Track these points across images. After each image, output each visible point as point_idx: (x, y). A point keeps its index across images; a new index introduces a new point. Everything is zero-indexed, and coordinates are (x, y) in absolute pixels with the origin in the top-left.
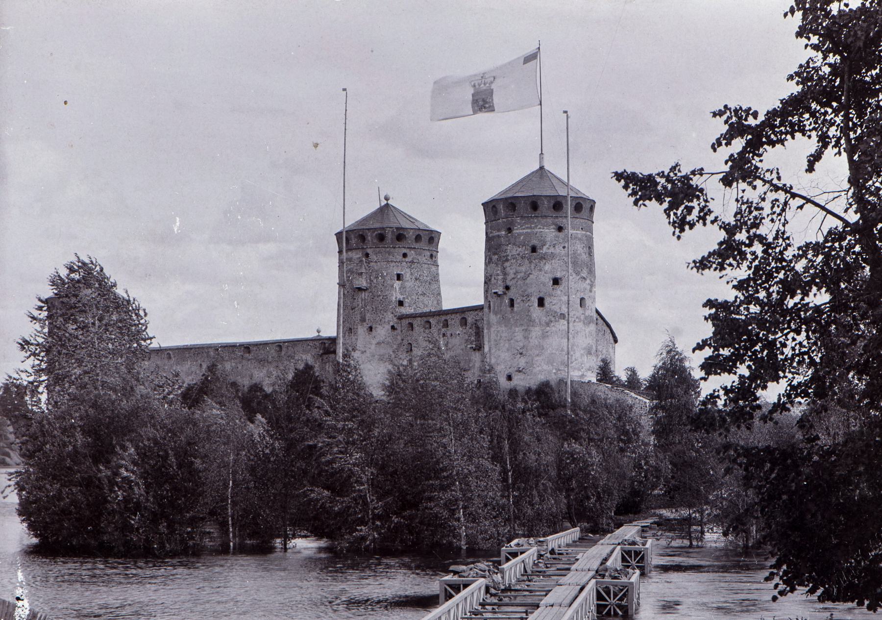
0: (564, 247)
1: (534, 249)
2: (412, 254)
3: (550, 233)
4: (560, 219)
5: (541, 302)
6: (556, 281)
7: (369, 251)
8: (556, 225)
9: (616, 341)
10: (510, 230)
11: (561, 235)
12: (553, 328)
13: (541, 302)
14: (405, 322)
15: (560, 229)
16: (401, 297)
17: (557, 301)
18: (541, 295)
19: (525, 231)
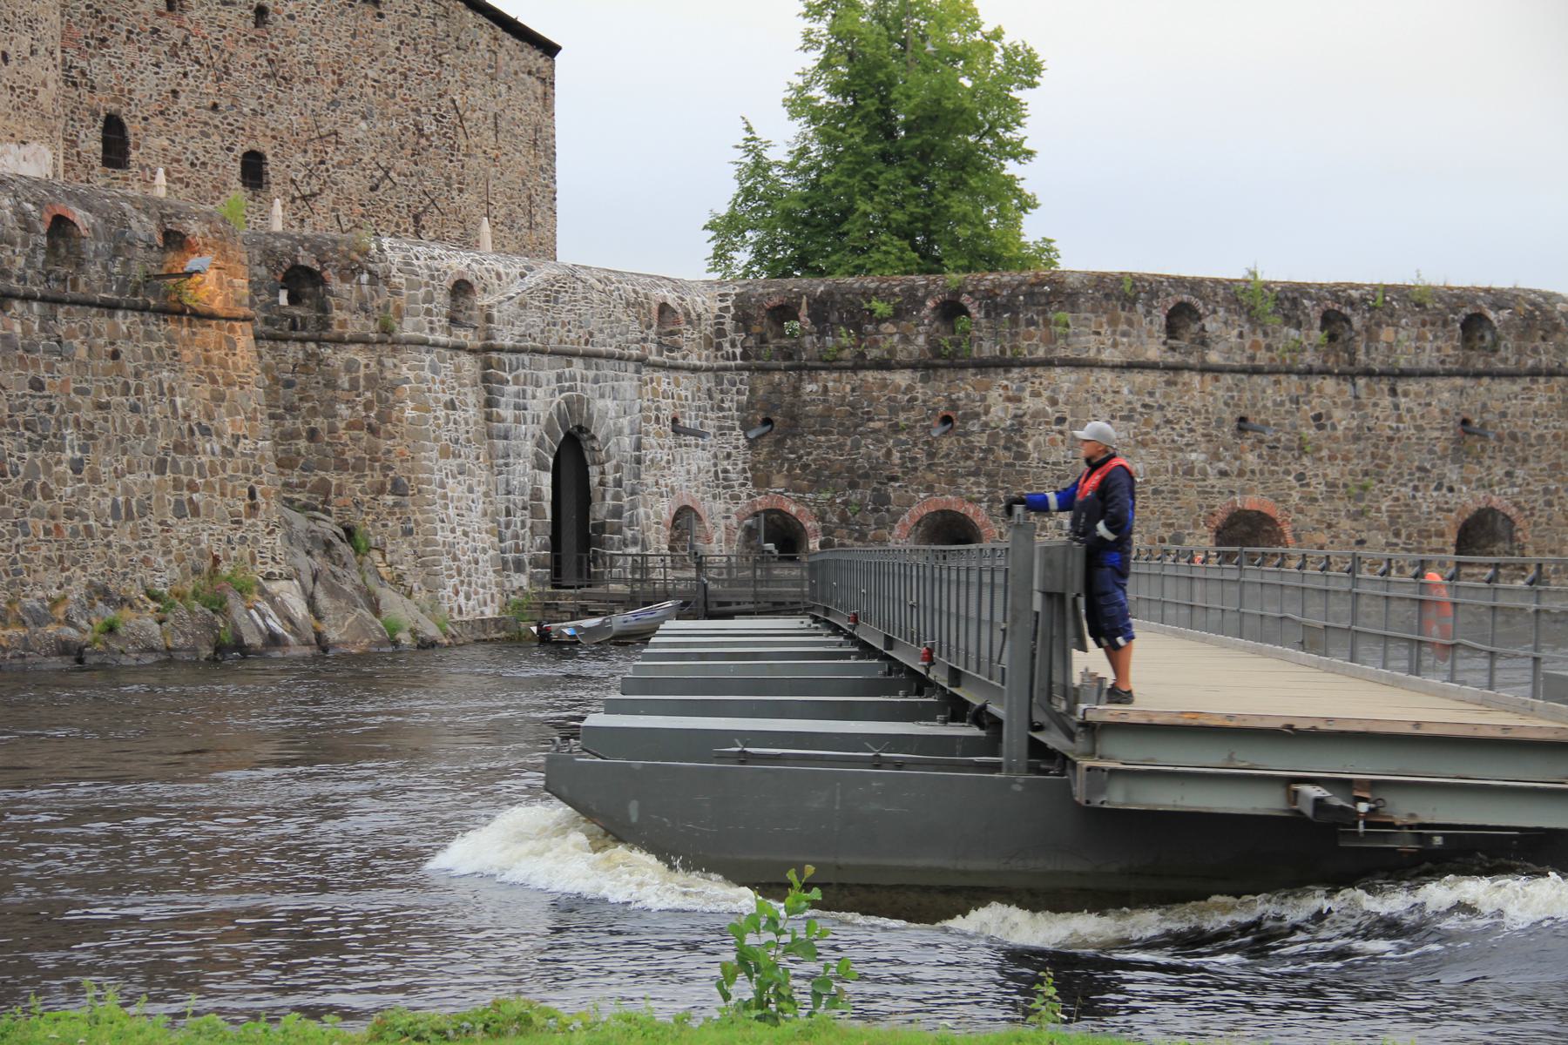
9: (550, 49)
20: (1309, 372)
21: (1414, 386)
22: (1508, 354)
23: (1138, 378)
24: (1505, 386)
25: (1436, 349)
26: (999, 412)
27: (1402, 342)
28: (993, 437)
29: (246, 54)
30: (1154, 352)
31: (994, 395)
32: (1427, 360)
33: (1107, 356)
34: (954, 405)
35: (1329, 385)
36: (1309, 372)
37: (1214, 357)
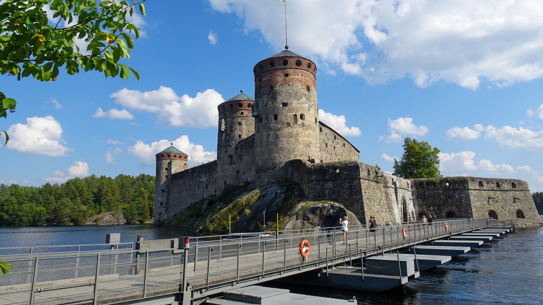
0: (289, 85)
1: (272, 87)
5: (276, 118)
6: (285, 105)
7: (226, 113)
9: (359, 152)
11: (287, 78)
17: (286, 115)
20: (496, 190)
21: (508, 192)
22: (517, 189)
23: (476, 191)
24: (518, 192)
25: (509, 187)
26: (457, 196)
27: (506, 186)
28: (457, 200)
29: (333, 152)
30: (478, 188)
31: (456, 194)
32: (509, 189)
33: (472, 188)
34: (450, 195)
35: (498, 192)
36: (496, 190)
37: (485, 188)
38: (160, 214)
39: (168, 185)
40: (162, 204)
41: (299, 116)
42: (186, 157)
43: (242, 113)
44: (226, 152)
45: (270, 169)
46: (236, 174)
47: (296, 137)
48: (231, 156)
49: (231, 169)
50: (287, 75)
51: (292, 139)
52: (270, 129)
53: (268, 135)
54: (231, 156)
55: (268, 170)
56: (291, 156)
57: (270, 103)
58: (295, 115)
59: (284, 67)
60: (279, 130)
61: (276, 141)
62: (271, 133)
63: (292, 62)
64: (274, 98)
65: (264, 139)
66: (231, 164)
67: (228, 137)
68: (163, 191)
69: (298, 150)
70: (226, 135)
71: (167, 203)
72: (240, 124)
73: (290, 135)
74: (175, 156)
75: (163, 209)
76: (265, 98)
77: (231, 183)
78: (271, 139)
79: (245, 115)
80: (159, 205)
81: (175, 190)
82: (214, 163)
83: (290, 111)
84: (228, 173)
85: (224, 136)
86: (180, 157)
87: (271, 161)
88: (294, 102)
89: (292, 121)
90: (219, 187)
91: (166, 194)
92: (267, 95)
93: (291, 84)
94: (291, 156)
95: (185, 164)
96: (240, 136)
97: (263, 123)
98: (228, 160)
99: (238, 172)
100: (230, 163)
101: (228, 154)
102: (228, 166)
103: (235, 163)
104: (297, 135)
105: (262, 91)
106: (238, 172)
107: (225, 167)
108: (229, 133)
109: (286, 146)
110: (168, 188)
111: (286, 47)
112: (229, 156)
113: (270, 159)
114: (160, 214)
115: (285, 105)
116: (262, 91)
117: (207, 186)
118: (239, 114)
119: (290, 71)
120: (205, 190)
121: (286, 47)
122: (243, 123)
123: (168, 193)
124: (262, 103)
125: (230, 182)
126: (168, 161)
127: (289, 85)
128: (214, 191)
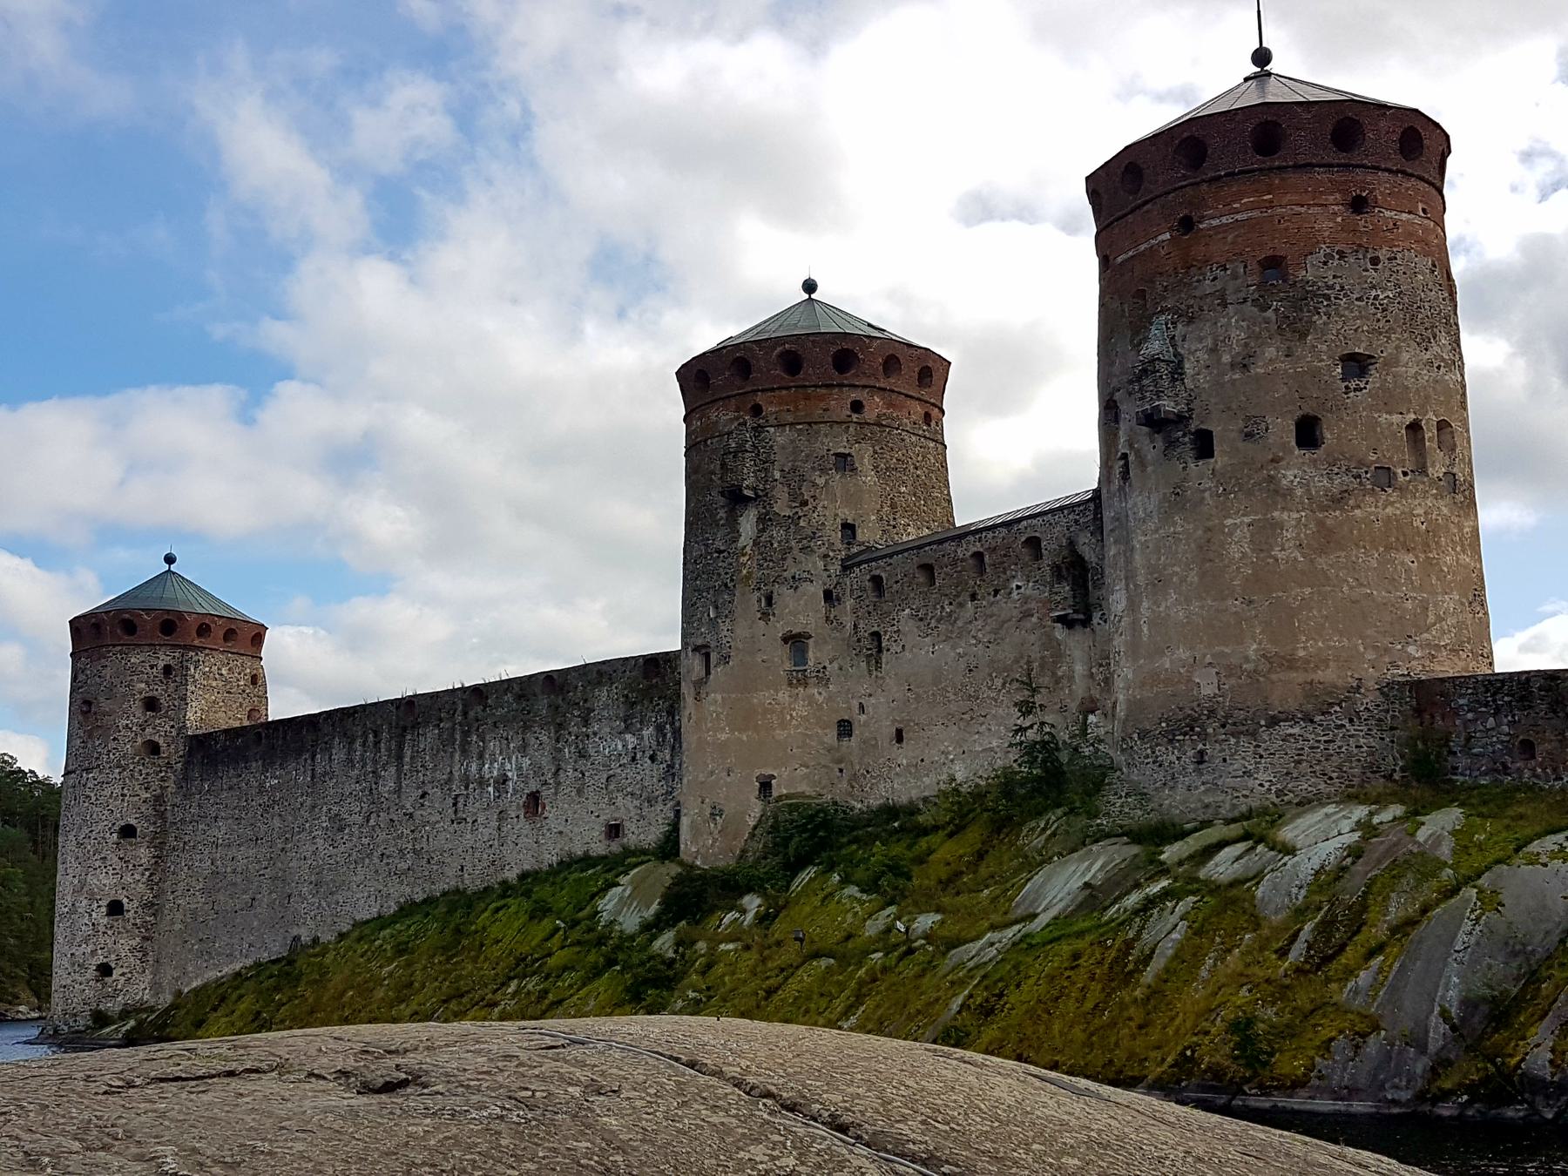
0: (1375, 261)
2: (875, 406)
3: (1328, 217)
4: (1359, 174)
5: (1308, 433)
6: (1357, 365)
7: (760, 399)
8: (1344, 192)
10: (1187, 224)
11: (1361, 222)
12: (1357, 512)
13: (1308, 433)
14: (860, 576)
15: (1359, 205)
16: (848, 514)
18: (1307, 410)
19: (1239, 217)
38: (105, 970)
39: (159, 800)
40: (115, 908)
41: (1430, 433)
42: (257, 635)
43: (857, 407)
44: (765, 616)
45: (1291, 718)
46: (831, 736)
47: (1426, 547)
48: (796, 641)
49: (801, 709)
50: (1359, 205)
51: (1408, 558)
52: (1278, 494)
53: (1266, 532)
54: (796, 641)
55: (1273, 722)
56: (1411, 649)
57: (1270, 352)
58: (1414, 427)
59: (1342, 158)
60: (1339, 500)
61: (1322, 562)
62: (1288, 517)
63: (1382, 138)
64: (1295, 329)
65: (1238, 547)
66: (803, 682)
67: (777, 533)
68: (128, 832)
69: (1440, 619)
70: (764, 521)
71: (153, 907)
72: (844, 462)
73: (1398, 536)
74: (203, 630)
75: (126, 944)
76: (1235, 328)
77: (803, 788)
78: (1286, 552)
79: (870, 414)
80: (100, 916)
81: (220, 832)
82: (653, 671)
83: (1388, 401)
84: (780, 734)
85: (748, 524)
86: (230, 635)
87: (1298, 677)
88: (1405, 356)
89: (1401, 460)
90: (716, 812)
91: (144, 854)
92: (1249, 308)
93: (1383, 254)
94: (1411, 649)
95: (255, 680)
96: (849, 529)
97: (1220, 460)
98: (781, 657)
99: (845, 728)
100: (799, 679)
101: (780, 627)
102: (784, 696)
103: (823, 679)
104: (1433, 530)
105: (1208, 286)
106: (845, 728)
107: (763, 697)
108: (782, 507)
109: (1380, 594)
110: (162, 815)
111: (1262, 57)
112: (785, 640)
113: (1290, 663)
114: (105, 970)
115: (1357, 365)
116: (1208, 286)
117: (533, 803)
118: (839, 406)
119: (1381, 185)
120: (523, 825)
121: (1262, 57)
122: (865, 461)
123: (159, 844)
124: (1213, 350)
125: (793, 781)
126: (164, 659)
127: (1375, 261)
128: (597, 832)
